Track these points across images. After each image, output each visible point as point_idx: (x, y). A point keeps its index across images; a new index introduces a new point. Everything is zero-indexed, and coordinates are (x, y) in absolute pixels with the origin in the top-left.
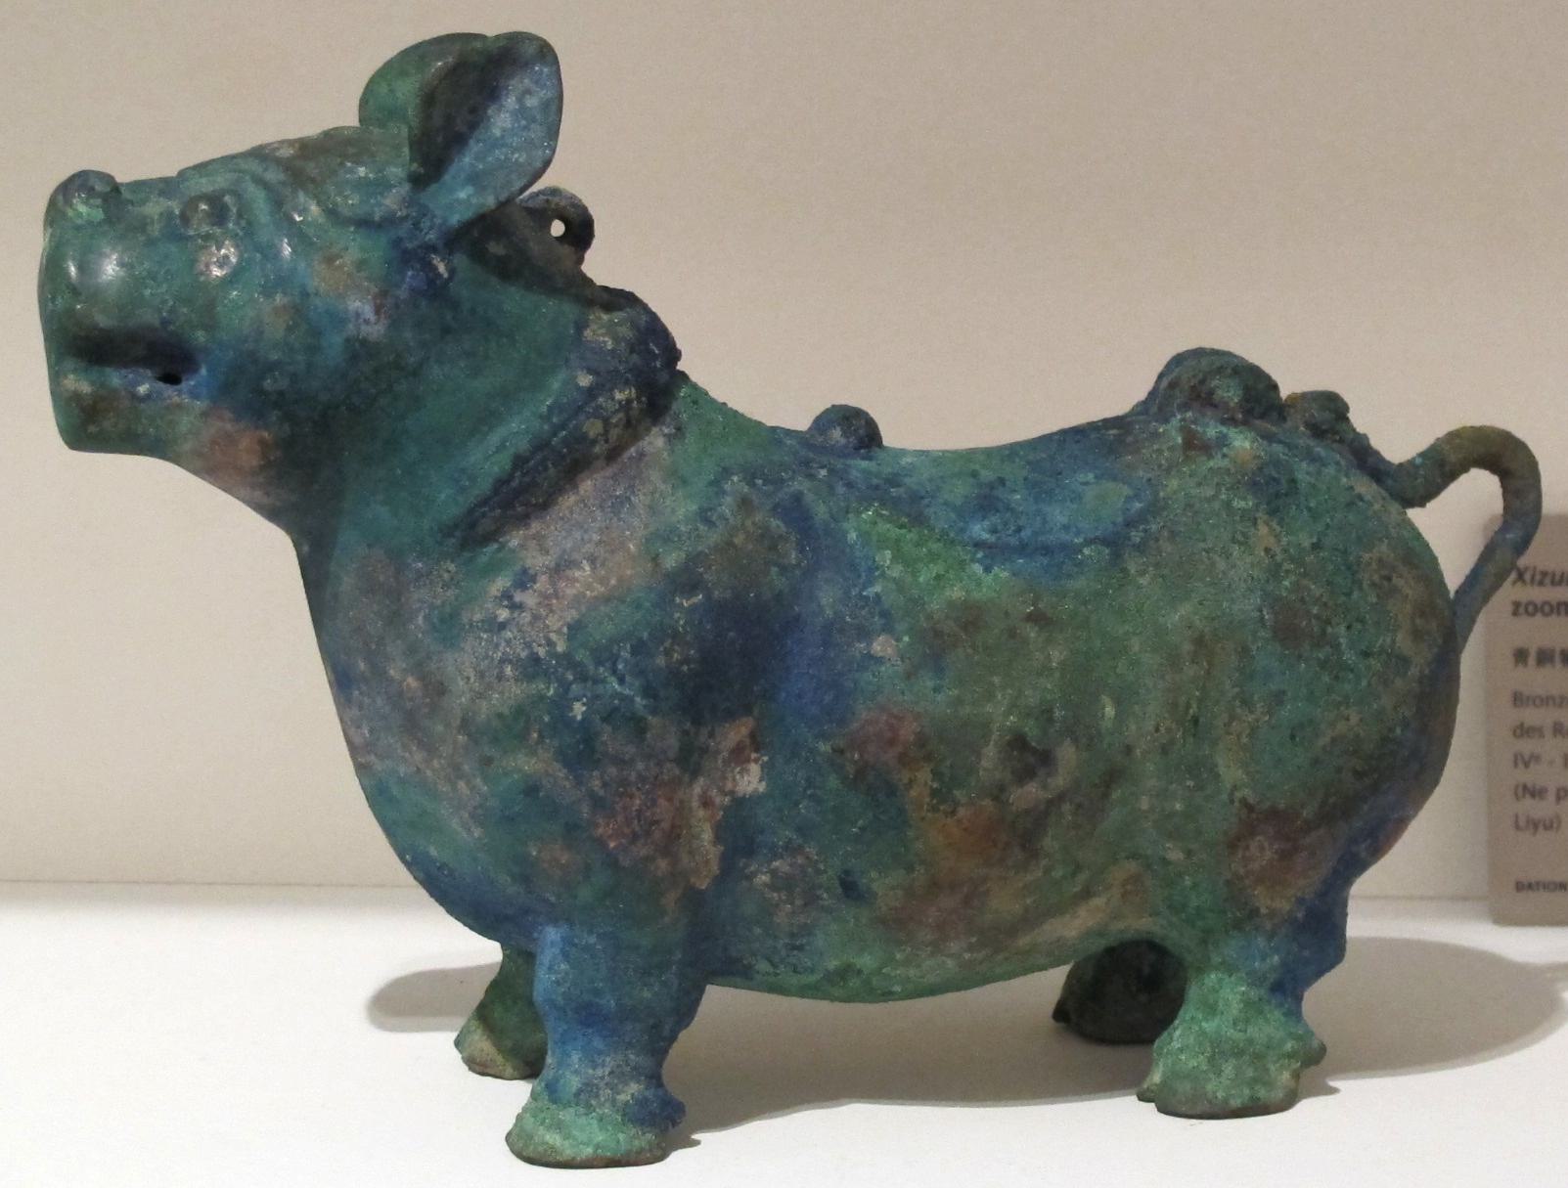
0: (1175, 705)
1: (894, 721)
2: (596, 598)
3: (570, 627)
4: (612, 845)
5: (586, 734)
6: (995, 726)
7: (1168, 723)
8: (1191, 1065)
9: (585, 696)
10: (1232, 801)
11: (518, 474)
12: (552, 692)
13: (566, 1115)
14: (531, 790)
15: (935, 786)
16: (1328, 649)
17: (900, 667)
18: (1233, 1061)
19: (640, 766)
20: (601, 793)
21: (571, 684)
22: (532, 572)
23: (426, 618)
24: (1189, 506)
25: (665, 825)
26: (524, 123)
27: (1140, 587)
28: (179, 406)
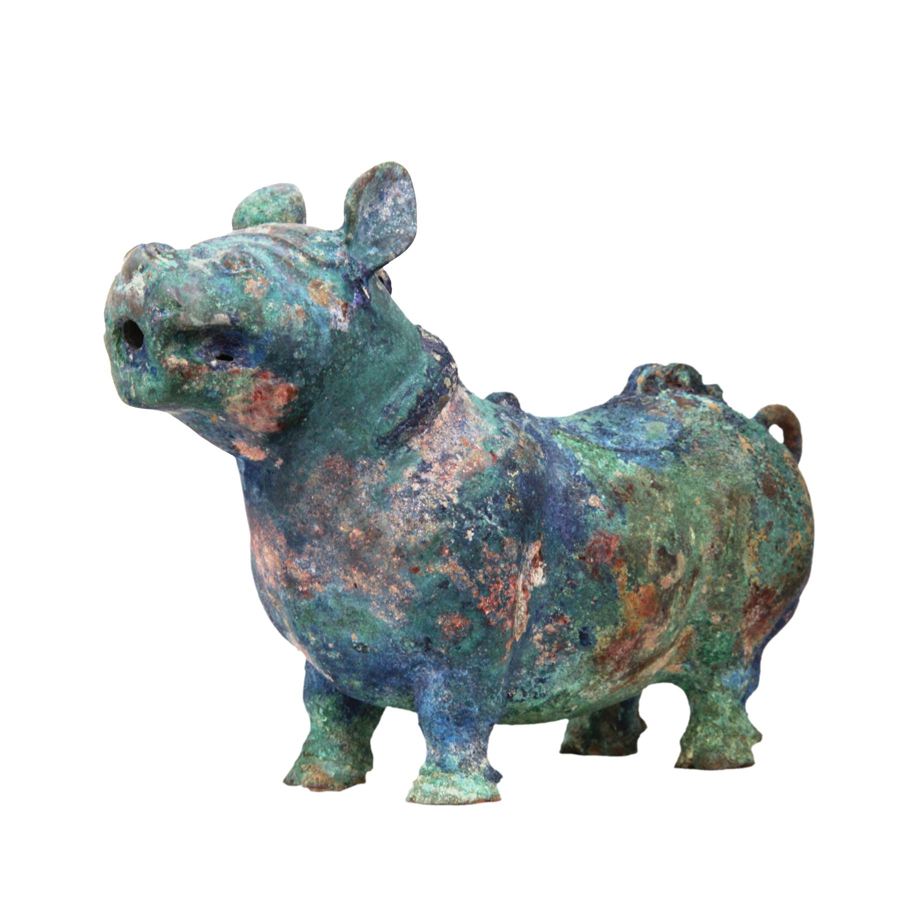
0: (721, 532)
1: (608, 541)
2: (469, 473)
3: (458, 489)
4: (487, 612)
5: (475, 547)
6: (652, 543)
7: (718, 542)
8: (713, 744)
9: (473, 527)
10: (749, 585)
11: (419, 407)
12: (454, 526)
13: (455, 778)
14: (444, 584)
15: (629, 575)
16: (786, 500)
17: (606, 512)
18: (734, 739)
19: (502, 566)
20: (483, 582)
21: (464, 520)
22: (428, 462)
23: (367, 493)
24: (703, 430)
25: (512, 600)
26: (398, 213)
27: (692, 471)
28: (237, 372)
